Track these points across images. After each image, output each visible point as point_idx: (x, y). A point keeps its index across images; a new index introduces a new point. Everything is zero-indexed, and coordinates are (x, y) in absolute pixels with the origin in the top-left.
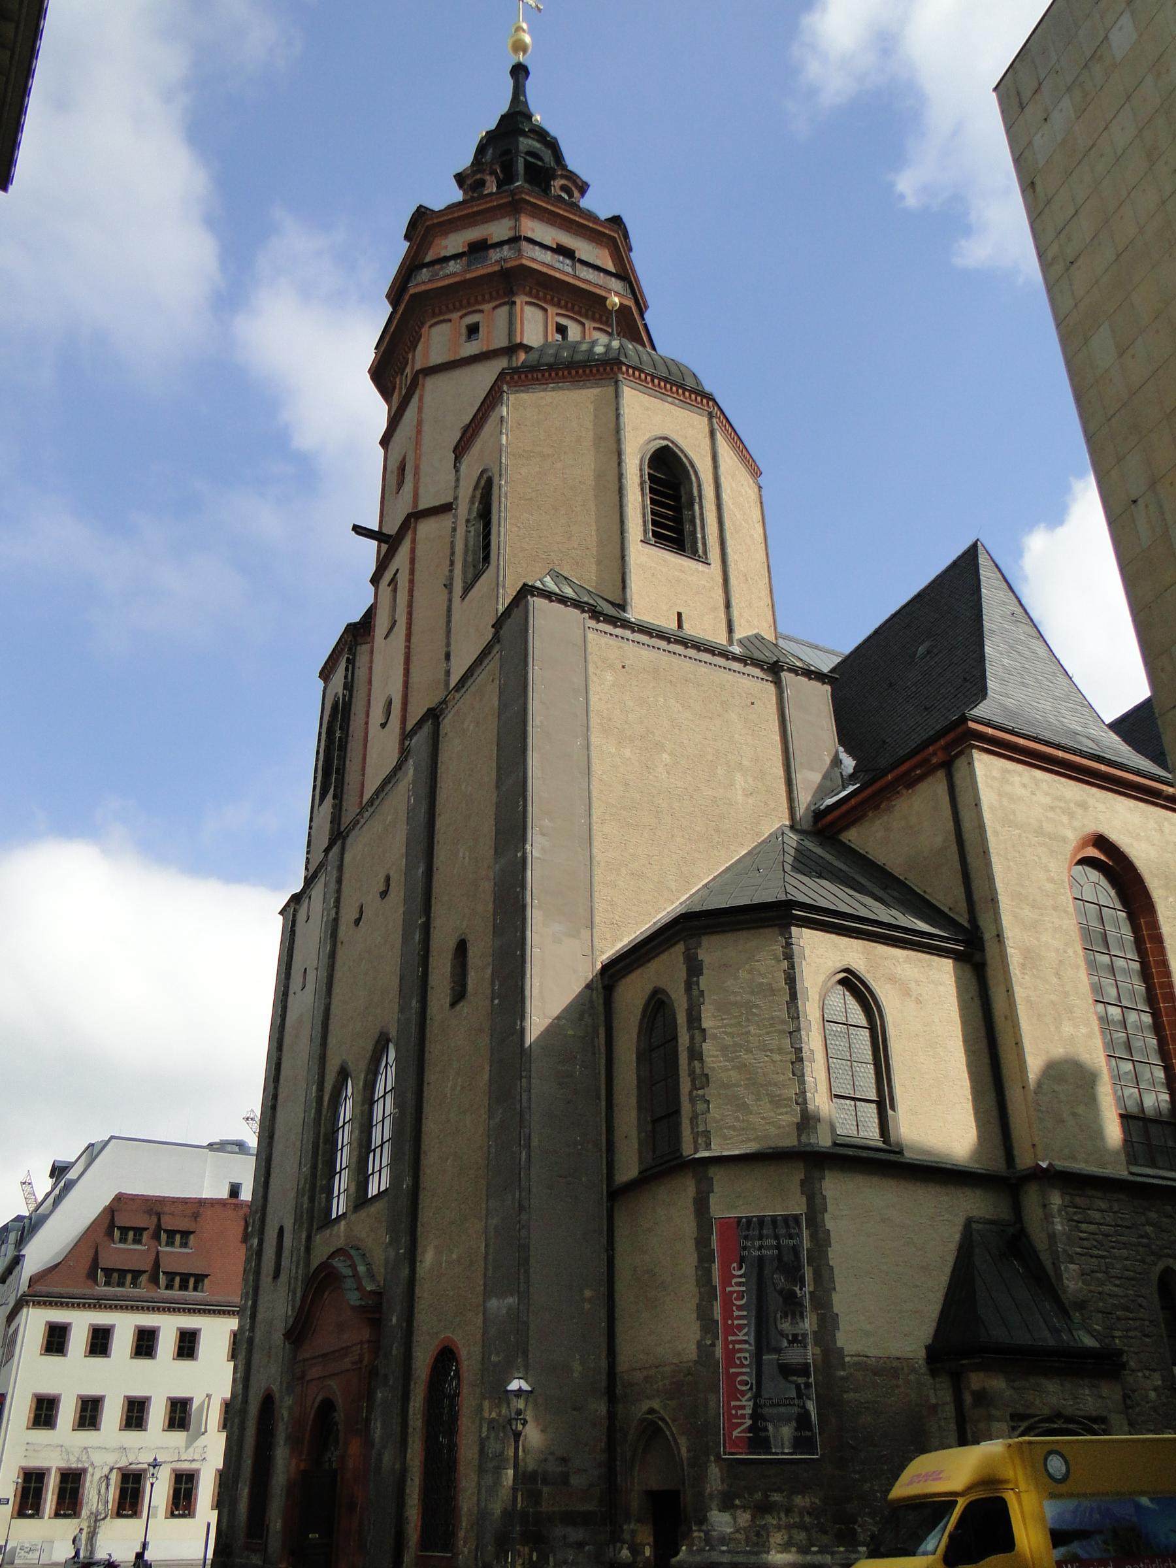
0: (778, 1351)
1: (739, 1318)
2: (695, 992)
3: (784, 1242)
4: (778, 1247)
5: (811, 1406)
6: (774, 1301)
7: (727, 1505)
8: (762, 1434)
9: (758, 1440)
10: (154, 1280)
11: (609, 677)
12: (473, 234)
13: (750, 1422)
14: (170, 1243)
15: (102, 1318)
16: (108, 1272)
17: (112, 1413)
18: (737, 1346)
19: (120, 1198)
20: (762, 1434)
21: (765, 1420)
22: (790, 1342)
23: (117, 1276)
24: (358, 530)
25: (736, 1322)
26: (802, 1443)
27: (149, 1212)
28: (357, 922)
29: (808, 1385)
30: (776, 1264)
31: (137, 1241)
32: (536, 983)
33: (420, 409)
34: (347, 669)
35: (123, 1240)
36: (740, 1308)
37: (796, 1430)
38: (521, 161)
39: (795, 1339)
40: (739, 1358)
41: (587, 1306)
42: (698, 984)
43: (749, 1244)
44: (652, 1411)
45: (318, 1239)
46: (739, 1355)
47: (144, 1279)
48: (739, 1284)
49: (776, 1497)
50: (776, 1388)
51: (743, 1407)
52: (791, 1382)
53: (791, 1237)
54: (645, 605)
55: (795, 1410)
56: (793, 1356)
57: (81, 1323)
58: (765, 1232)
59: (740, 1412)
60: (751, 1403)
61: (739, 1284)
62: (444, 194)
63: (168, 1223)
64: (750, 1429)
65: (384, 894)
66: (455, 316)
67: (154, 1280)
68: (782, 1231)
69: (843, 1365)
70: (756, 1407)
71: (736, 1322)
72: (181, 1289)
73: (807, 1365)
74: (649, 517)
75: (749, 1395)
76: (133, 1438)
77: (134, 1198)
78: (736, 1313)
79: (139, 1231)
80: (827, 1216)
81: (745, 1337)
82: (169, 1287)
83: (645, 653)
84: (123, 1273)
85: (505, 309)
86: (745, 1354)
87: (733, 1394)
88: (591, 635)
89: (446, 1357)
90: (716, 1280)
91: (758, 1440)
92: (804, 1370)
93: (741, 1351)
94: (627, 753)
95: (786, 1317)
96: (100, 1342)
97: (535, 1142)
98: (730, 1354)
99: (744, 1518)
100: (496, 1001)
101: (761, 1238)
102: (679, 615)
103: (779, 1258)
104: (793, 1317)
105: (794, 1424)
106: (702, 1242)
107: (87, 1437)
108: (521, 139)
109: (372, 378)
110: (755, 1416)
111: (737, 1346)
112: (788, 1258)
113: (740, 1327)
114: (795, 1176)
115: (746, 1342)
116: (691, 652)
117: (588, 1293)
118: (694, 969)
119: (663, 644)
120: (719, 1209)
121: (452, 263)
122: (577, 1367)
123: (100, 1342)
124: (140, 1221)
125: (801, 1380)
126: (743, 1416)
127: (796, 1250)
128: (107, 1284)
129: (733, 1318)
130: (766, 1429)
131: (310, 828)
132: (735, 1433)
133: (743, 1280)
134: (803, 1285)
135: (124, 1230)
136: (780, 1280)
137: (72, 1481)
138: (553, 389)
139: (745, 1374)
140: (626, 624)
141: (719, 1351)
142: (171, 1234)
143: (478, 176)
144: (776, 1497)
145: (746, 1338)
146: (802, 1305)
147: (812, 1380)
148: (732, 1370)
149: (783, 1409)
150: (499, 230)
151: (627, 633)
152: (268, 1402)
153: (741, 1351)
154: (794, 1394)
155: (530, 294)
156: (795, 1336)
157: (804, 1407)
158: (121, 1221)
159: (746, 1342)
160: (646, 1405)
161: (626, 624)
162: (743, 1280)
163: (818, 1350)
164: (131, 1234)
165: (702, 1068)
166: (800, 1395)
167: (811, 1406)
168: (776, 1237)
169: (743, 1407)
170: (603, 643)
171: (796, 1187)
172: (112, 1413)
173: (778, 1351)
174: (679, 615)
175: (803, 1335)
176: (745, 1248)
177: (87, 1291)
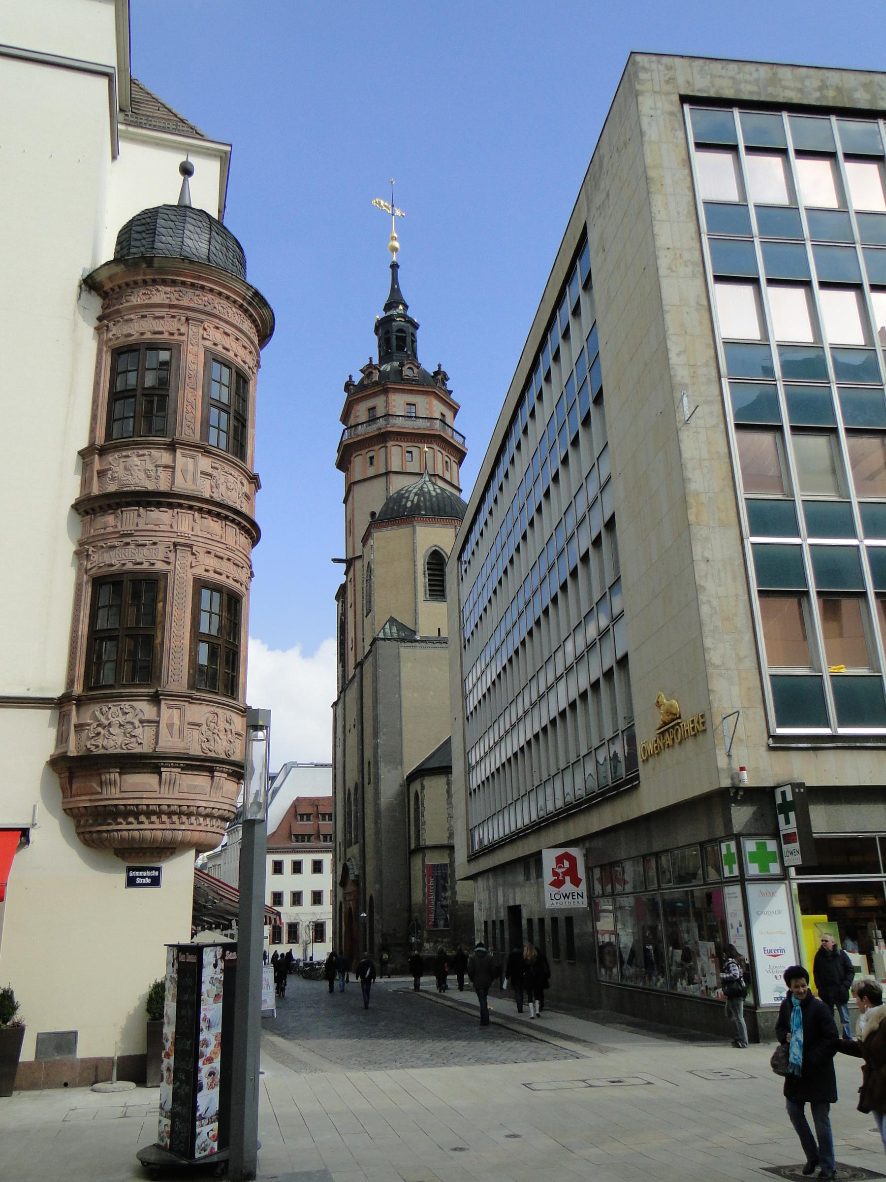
7: (428, 942)
9: (435, 924)
10: (318, 838)
11: (409, 665)
12: (370, 403)
14: (324, 820)
15: (297, 857)
16: (296, 836)
17: (307, 898)
19: (298, 799)
23: (300, 838)
24: (335, 560)
26: (446, 925)
31: (308, 820)
33: (353, 504)
35: (302, 820)
38: (394, 337)
39: (445, 898)
45: (348, 850)
47: (312, 838)
54: (425, 630)
56: (444, 903)
57: (287, 860)
62: (357, 378)
63: (322, 810)
66: (364, 452)
67: (318, 838)
74: (428, 588)
77: (305, 799)
79: (308, 815)
81: (433, 897)
82: (325, 841)
84: (303, 836)
89: (371, 897)
91: (435, 924)
92: (446, 906)
94: (416, 695)
96: (297, 867)
97: (383, 839)
98: (429, 902)
99: (432, 944)
106: (423, 871)
107: (297, 909)
118: (423, 788)
119: (431, 645)
120: (427, 863)
123: (297, 867)
124: (309, 810)
127: (446, 874)
128: (297, 841)
135: (302, 815)
137: (293, 928)
139: (433, 908)
140: (416, 641)
142: (324, 815)
150: (379, 402)
151: (417, 644)
152: (341, 904)
155: (394, 440)
158: (301, 811)
161: (416, 641)
170: (406, 651)
172: (307, 898)
177: (288, 845)
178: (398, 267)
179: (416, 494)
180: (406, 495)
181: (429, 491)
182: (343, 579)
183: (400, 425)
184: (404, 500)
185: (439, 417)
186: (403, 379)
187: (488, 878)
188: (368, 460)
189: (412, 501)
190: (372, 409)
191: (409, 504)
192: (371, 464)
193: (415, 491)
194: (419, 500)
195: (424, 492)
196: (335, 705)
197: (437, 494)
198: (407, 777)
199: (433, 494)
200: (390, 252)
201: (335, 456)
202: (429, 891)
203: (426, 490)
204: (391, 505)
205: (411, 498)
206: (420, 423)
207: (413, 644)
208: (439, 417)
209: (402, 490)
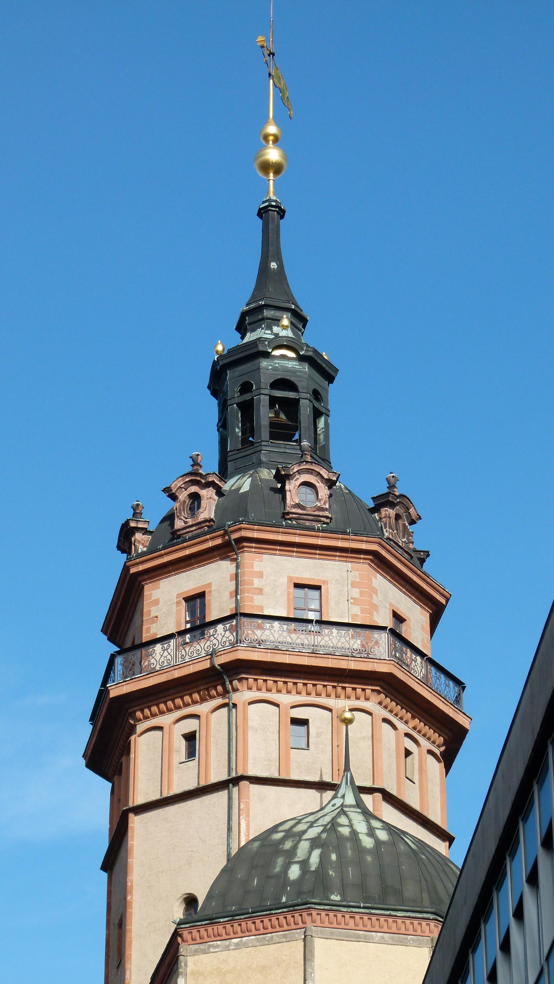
38: (265, 400)
85: (225, 710)
108: (264, 363)
109: (88, 766)
121: (158, 647)
138: (238, 947)
178: (282, 213)
179: (315, 843)
180: (288, 845)
181: (354, 834)
183: (273, 641)
184: (280, 861)
185: (387, 621)
186: (285, 515)
187: (228, 786)
188: (182, 744)
189: (304, 864)
190: (196, 600)
191: (294, 872)
192: (191, 753)
193: (313, 833)
194: (323, 858)
195: (340, 838)
197: (378, 842)
199: (367, 842)
200: (260, 174)
201: (81, 733)
203: (345, 831)
204: (240, 875)
205: (301, 853)
206: (333, 639)
208: (387, 621)
209: (274, 829)
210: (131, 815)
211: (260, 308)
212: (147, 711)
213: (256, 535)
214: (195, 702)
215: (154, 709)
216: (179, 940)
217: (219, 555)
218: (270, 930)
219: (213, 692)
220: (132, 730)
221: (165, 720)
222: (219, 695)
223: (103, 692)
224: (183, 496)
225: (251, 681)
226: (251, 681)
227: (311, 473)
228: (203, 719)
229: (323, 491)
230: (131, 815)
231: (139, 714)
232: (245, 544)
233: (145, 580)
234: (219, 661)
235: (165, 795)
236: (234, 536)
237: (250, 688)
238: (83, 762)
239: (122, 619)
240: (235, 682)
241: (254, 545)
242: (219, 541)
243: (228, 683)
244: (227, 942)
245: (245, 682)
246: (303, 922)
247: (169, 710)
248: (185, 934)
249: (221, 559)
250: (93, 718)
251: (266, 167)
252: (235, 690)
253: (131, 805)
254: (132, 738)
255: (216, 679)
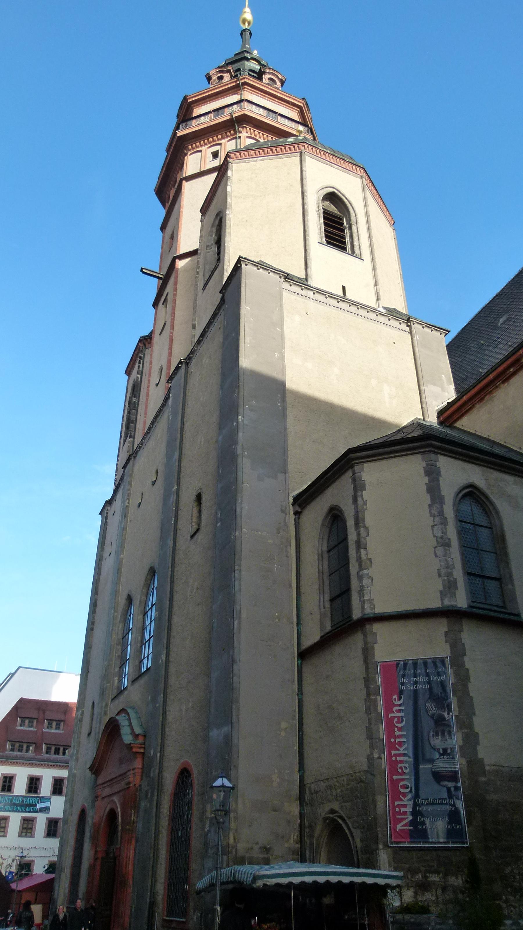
0: (432, 761)
1: (400, 736)
2: (360, 502)
3: (434, 678)
4: (429, 682)
5: (460, 805)
6: (427, 724)
8: (421, 827)
9: (418, 831)
13: (411, 818)
18: (399, 759)
20: (421, 827)
21: (423, 816)
22: (441, 754)
25: (398, 740)
27: (39, 709)
28: (139, 505)
29: (457, 788)
30: (427, 696)
32: (246, 507)
34: (140, 363)
36: (400, 729)
37: (450, 823)
39: (445, 752)
40: (401, 768)
41: (283, 734)
42: (362, 496)
43: (406, 680)
44: (332, 811)
46: (399, 765)
48: (399, 711)
49: (434, 878)
50: (431, 790)
51: (405, 806)
52: (442, 786)
53: (438, 674)
55: (447, 808)
56: (444, 765)
58: (418, 671)
59: (402, 810)
60: (411, 803)
61: (399, 711)
63: (49, 715)
64: (411, 823)
65: (154, 483)
68: (431, 670)
69: (484, 773)
70: (415, 805)
71: (398, 740)
72: (55, 753)
73: (456, 772)
75: (409, 796)
76: (26, 842)
78: (397, 733)
79: (31, 719)
80: (466, 660)
81: (406, 749)
83: (321, 308)
85: (235, 140)
86: (406, 763)
87: (396, 795)
88: (285, 294)
89: (184, 774)
90: (381, 708)
91: (418, 831)
92: (453, 777)
93: (402, 762)
95: (437, 734)
98: (393, 766)
100: (219, 524)
101: (415, 676)
102: (344, 288)
103: (430, 689)
104: (443, 734)
105: (447, 819)
106: (368, 681)
108: (246, 63)
109: (156, 194)
110: (415, 813)
111: (399, 759)
112: (437, 690)
113: (401, 744)
114: (441, 626)
115: (405, 755)
116: (353, 309)
117: (284, 725)
122: (275, 779)
125: (451, 784)
126: (405, 813)
127: (443, 685)
128: (13, 750)
129: (395, 737)
130: (423, 823)
131: (118, 461)
132: (399, 827)
133: (402, 708)
134: (450, 710)
136: (431, 707)
139: (407, 780)
140: (309, 288)
141: (384, 763)
143: (220, 75)
144: (434, 878)
145: (406, 752)
146: (449, 726)
147: (460, 784)
148: (395, 777)
149: (437, 808)
152: (83, 814)
153: (402, 762)
154: (446, 796)
156: (445, 750)
157: (454, 805)
159: (405, 755)
160: (327, 807)
161: (309, 288)
162: (402, 708)
163: (464, 761)
164: (27, 721)
165: (367, 554)
166: (450, 796)
167: (460, 805)
168: (427, 675)
169: (405, 806)
171: (442, 638)
173: (432, 761)
174: (344, 288)
175: (451, 748)
176: (403, 684)
178: (251, 34)
182: (144, 322)
196: (109, 503)
198: (297, 499)
202: (390, 733)
207: (305, 292)
210: (184, 182)
211: (243, 52)
212: (194, 145)
213: (251, 83)
214: (219, 139)
215: (198, 144)
216: (228, 159)
217: (232, 92)
218: (280, 153)
219: (228, 134)
220: (186, 155)
221: (203, 148)
222: (231, 135)
223: (174, 134)
224: (214, 78)
225: (248, 129)
226: (248, 129)
227: (274, 76)
228: (223, 145)
229: (279, 84)
230: (184, 182)
231: (190, 147)
232: (246, 86)
233: (194, 106)
234: (234, 116)
235: (202, 170)
236: (241, 82)
237: (247, 132)
238: (154, 193)
239: (185, 113)
240: (240, 129)
241: (249, 88)
242: (234, 84)
243: (237, 128)
244: (256, 159)
245: (245, 129)
246: (299, 149)
247: (205, 144)
248: (232, 155)
249: (233, 95)
250: (168, 150)
251: (244, 21)
252: (240, 132)
253: (184, 176)
254: (186, 157)
255: (231, 126)
